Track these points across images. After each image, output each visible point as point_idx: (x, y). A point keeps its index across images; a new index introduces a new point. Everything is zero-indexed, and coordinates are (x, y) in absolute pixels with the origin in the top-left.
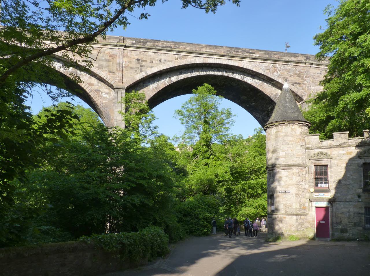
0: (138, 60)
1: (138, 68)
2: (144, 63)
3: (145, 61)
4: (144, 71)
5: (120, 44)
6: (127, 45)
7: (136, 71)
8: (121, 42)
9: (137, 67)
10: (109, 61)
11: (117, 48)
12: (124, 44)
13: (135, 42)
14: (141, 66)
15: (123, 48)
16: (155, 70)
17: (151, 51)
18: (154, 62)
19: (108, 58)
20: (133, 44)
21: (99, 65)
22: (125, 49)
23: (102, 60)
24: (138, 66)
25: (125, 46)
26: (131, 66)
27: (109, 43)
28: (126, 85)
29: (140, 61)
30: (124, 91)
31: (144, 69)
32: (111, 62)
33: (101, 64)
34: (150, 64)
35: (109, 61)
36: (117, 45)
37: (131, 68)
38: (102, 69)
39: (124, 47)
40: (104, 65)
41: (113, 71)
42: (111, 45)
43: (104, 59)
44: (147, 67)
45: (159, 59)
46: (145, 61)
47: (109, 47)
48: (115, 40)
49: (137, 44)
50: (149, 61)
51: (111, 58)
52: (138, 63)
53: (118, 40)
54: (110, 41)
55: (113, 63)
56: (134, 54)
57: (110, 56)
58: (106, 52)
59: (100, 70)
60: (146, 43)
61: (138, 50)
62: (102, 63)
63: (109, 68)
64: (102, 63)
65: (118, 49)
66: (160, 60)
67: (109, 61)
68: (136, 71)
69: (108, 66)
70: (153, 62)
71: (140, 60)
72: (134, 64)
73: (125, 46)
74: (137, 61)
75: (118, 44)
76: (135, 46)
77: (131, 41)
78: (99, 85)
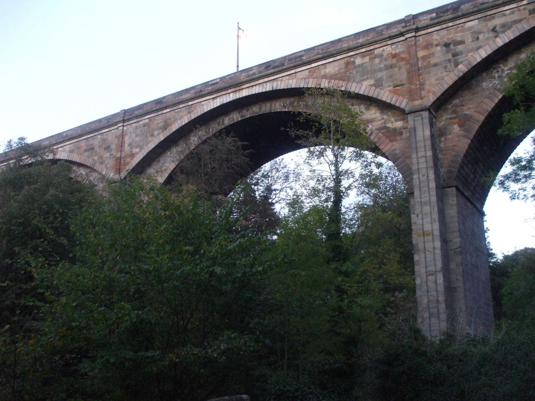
0: (447, 45)
1: (449, 61)
2: (460, 48)
3: (462, 42)
4: (462, 62)
5: (407, 28)
6: (420, 26)
7: (445, 67)
8: (410, 25)
9: (446, 60)
10: (392, 66)
11: (403, 38)
12: (414, 27)
13: (437, 14)
14: (455, 55)
15: (413, 34)
16: (483, 54)
17: (472, 18)
18: (481, 37)
20: (432, 19)
21: (376, 81)
22: (417, 35)
23: (381, 70)
24: (449, 56)
25: (417, 30)
26: (433, 61)
27: (387, 36)
28: (430, 99)
29: (452, 46)
30: (426, 114)
31: (460, 59)
32: (396, 67)
34: (474, 45)
36: (402, 34)
37: (435, 65)
38: (382, 85)
39: (416, 32)
40: (384, 77)
41: (402, 83)
42: (391, 38)
43: (382, 66)
44: (469, 52)
45: (491, 28)
46: (462, 42)
47: (389, 42)
48: (399, 26)
49: (441, 17)
50: (469, 39)
51: (395, 61)
52: (448, 52)
53: (403, 24)
54: (389, 32)
55: (399, 69)
58: (385, 54)
59: (378, 90)
60: (459, 7)
61: (444, 26)
62: (379, 75)
63: (393, 80)
64: (379, 75)
65: (406, 39)
66: (494, 30)
67: (392, 66)
68: (445, 67)
69: (391, 77)
70: (478, 39)
71: (450, 44)
72: (439, 54)
73: (417, 30)
74: (444, 48)
75: (403, 30)
76: (436, 21)
77: (429, 17)
78: (385, 117)
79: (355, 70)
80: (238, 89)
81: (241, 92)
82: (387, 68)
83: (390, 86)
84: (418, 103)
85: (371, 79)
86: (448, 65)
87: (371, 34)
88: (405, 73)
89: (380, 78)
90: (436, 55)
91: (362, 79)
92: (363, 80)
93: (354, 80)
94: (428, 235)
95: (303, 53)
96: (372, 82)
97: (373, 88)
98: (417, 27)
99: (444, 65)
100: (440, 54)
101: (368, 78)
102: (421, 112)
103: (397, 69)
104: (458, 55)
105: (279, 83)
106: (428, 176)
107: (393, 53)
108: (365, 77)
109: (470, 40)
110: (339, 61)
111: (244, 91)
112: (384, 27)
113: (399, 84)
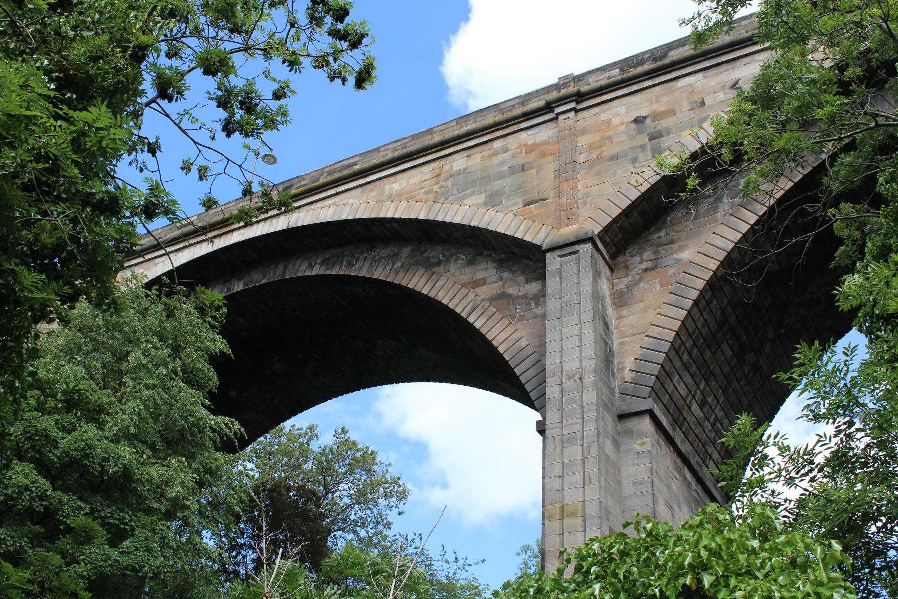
0: (638, 121)
1: (642, 147)
3: (672, 112)
7: (634, 161)
10: (523, 168)
19: (524, 159)
21: (490, 196)
23: (501, 176)
24: (644, 139)
28: (594, 219)
29: (648, 121)
31: (665, 142)
32: (531, 168)
33: (496, 188)
35: (523, 170)
37: (613, 158)
39: (578, 103)
40: (507, 189)
41: (542, 196)
43: (506, 168)
46: (672, 112)
51: (531, 157)
52: (640, 132)
56: (623, 110)
57: (529, 152)
59: (492, 212)
64: (497, 185)
70: (703, 103)
74: (633, 126)
79: (451, 180)
80: (224, 230)
81: (229, 236)
82: (513, 171)
83: (516, 204)
84: (568, 231)
85: (481, 193)
86: (641, 157)
87: (491, 115)
88: (551, 176)
89: (498, 190)
90: (615, 139)
91: (462, 195)
92: (466, 197)
93: (447, 198)
94: (572, 514)
95: (356, 159)
96: (482, 198)
97: (483, 210)
98: (579, 90)
99: (631, 156)
100: (624, 137)
101: (473, 193)
102: (577, 247)
103: (534, 171)
104: (661, 136)
105: (302, 214)
106: (580, 379)
107: (530, 143)
108: (467, 192)
109: (686, 106)
110: (423, 168)
111: (236, 233)
112: (517, 101)
113: (536, 198)
